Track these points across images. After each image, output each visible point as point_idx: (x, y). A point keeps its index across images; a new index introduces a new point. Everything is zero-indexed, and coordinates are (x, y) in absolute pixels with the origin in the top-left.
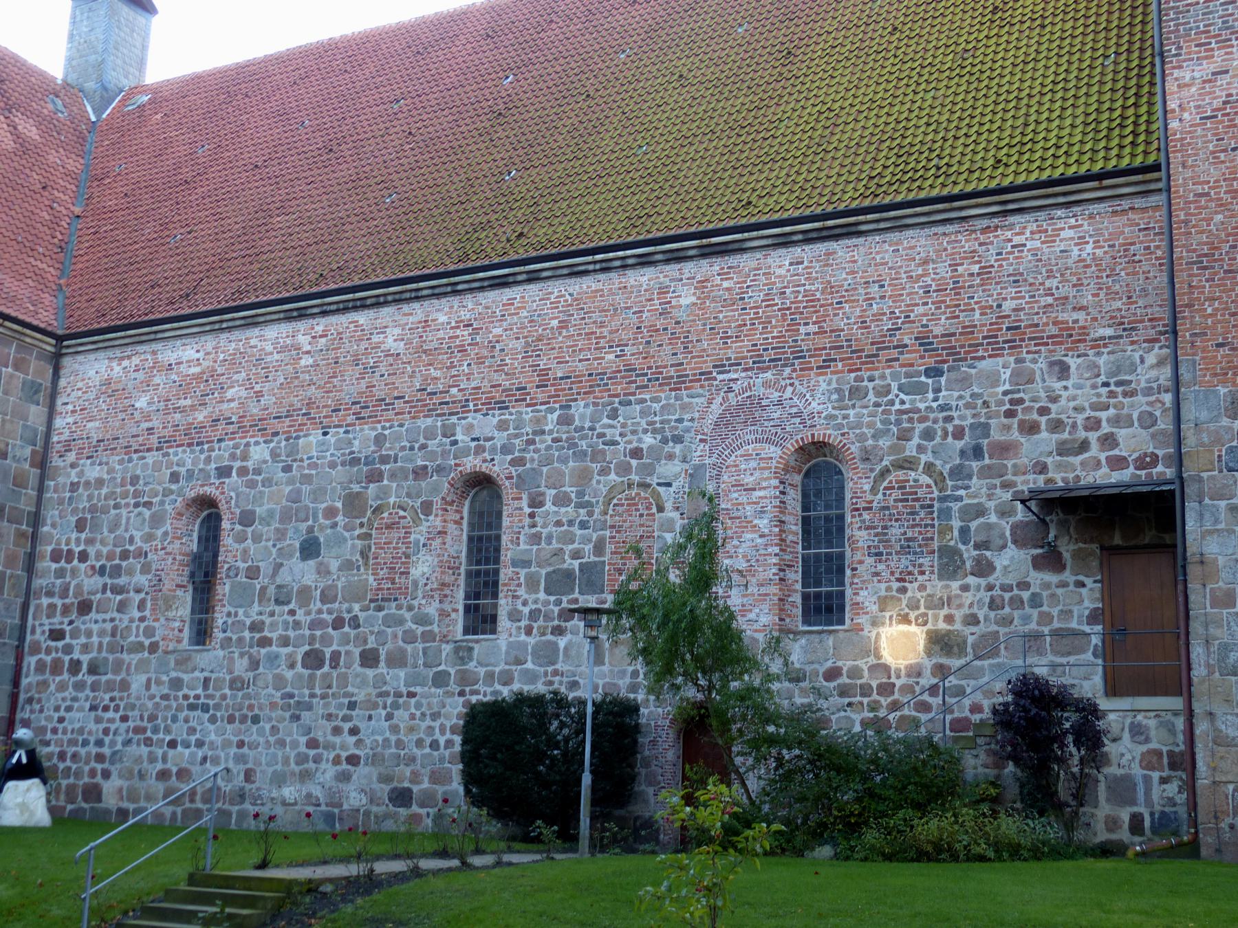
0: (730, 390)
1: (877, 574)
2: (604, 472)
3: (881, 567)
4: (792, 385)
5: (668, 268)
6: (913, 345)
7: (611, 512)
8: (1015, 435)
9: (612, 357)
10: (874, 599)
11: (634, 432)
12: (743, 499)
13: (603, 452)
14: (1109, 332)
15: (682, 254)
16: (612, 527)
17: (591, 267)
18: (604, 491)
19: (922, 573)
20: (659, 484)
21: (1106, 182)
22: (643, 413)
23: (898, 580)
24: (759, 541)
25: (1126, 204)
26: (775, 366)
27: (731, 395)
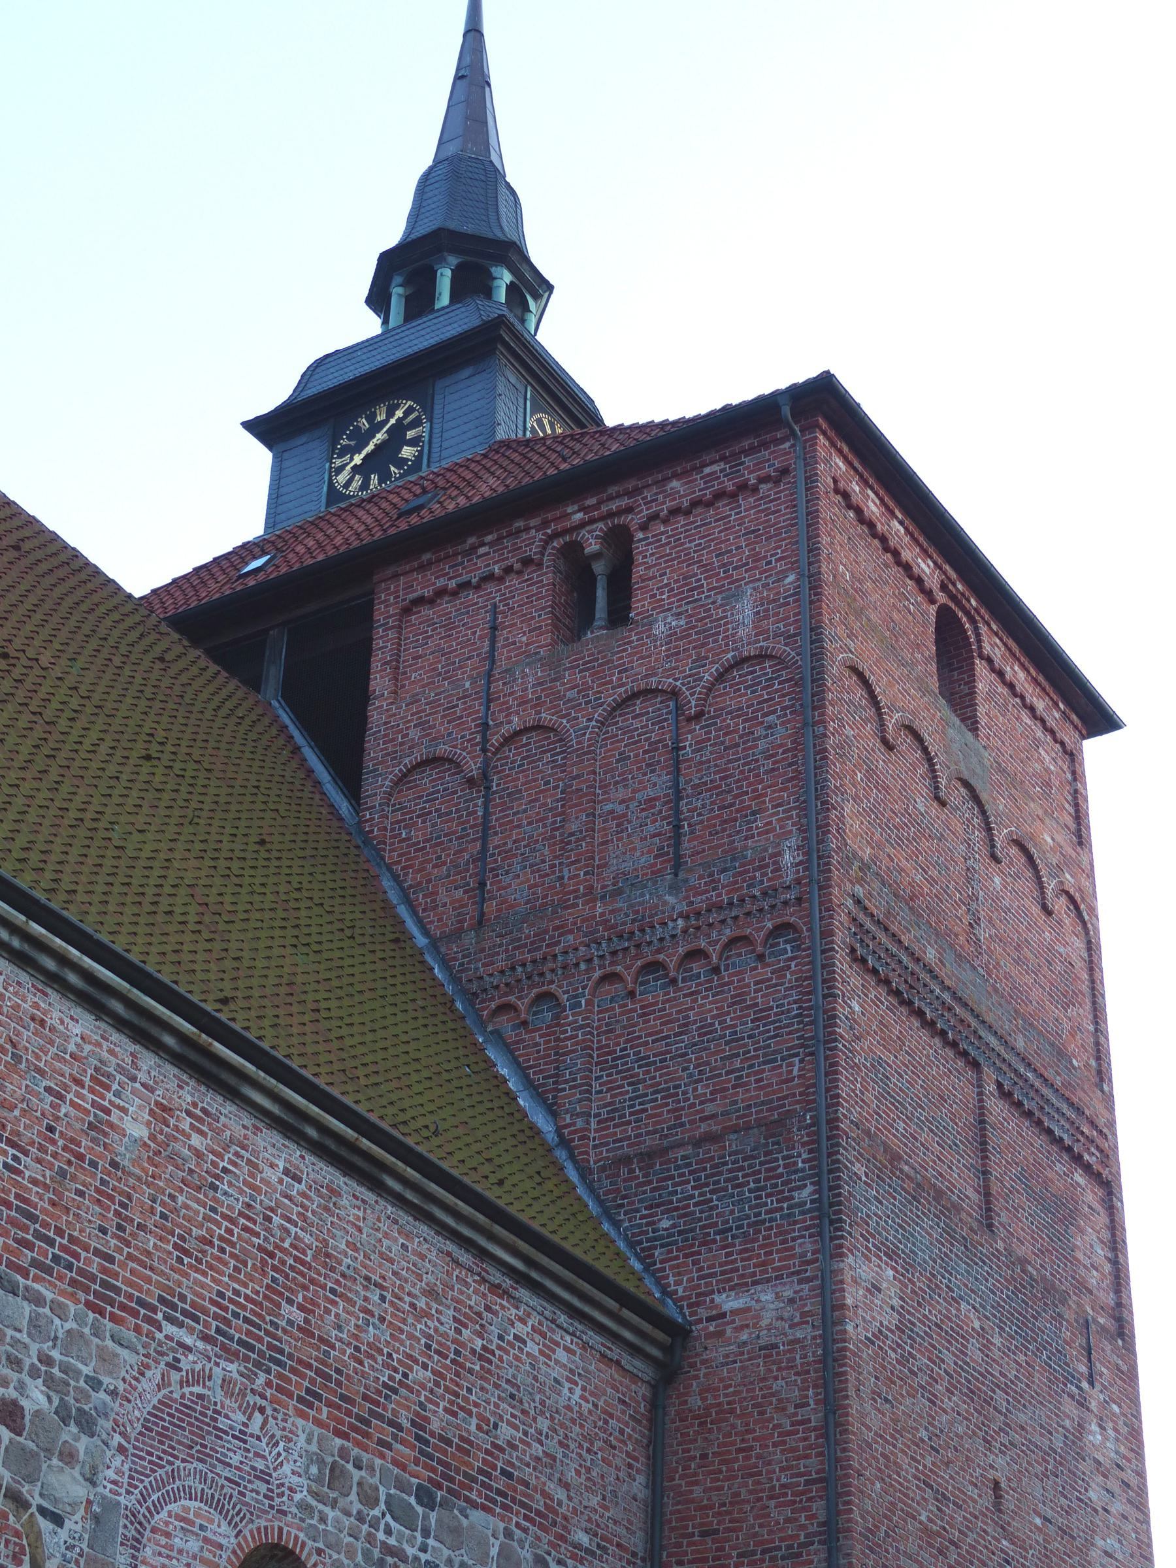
0: (174, 1366)
4: (262, 1410)
5: (115, 1037)
6: (409, 1432)
14: (584, 1539)
15: (155, 1031)
20: (42, 1511)
21: (626, 1313)
25: (615, 1353)
26: (246, 1359)
27: (175, 1376)
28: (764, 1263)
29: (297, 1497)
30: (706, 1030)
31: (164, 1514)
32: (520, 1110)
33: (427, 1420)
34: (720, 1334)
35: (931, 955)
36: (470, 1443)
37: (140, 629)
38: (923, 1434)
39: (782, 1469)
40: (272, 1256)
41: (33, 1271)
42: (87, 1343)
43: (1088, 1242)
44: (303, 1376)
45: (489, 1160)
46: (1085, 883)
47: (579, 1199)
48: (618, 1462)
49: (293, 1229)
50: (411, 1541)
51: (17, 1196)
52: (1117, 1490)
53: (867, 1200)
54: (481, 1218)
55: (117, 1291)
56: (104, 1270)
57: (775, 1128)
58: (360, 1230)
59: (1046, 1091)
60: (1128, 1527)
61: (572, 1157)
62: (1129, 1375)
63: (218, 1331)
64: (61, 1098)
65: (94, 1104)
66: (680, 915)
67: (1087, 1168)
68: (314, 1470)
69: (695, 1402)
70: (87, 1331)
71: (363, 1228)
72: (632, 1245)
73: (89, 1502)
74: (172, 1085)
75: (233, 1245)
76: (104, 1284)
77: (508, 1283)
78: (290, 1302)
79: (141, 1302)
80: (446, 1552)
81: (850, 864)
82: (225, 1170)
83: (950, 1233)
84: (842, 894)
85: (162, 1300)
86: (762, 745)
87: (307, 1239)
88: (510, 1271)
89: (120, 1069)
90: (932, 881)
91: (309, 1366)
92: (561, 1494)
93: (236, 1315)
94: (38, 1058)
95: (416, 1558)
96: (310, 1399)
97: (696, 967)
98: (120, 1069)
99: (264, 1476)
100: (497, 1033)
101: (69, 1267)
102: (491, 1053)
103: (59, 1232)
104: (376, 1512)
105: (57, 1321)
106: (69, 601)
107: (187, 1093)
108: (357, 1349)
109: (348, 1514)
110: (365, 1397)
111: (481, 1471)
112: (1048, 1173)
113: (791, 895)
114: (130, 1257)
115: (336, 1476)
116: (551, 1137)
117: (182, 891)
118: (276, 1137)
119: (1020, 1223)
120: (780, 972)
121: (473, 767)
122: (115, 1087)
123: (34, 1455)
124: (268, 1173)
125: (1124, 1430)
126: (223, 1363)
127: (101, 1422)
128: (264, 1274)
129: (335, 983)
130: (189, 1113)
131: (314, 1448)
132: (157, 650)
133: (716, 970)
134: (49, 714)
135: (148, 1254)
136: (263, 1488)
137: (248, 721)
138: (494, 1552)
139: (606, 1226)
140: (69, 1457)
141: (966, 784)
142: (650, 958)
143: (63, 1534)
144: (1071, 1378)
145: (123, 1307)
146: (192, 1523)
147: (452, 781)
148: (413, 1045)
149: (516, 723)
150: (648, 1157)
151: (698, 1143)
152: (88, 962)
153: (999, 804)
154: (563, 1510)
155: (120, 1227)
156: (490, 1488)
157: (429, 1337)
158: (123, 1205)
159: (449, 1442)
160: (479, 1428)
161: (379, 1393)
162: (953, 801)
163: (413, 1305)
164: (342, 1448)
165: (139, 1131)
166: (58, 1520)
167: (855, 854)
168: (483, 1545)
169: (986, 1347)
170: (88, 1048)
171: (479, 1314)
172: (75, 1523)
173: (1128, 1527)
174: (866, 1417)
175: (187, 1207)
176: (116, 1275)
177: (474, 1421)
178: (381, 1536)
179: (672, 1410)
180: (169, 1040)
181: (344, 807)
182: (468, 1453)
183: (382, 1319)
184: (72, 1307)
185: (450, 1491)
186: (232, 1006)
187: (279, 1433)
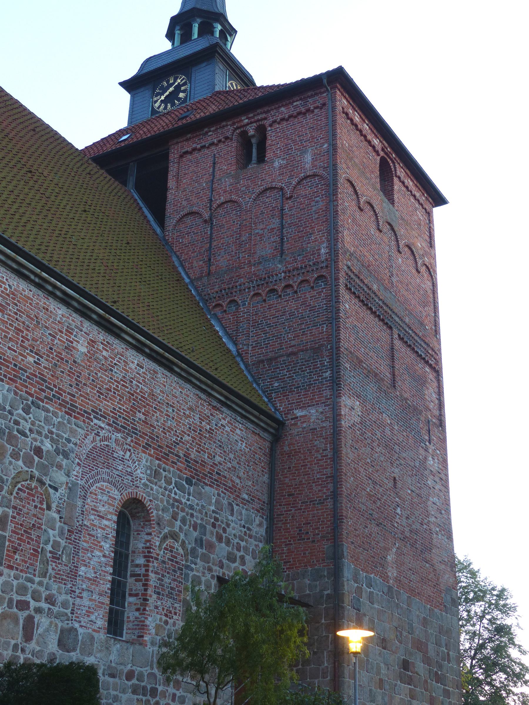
0: (98, 434)
1: (156, 607)
2: (15, 456)
3: (159, 603)
4: (130, 450)
5: (74, 315)
6: (183, 458)
7: (14, 493)
8: (214, 539)
9: (31, 360)
10: (154, 625)
11: (39, 433)
12: (96, 522)
13: (15, 436)
14: (246, 497)
15: (89, 313)
16: (15, 508)
17: (32, 277)
18: (13, 473)
19: (175, 614)
20: (50, 486)
21: (262, 417)
22: (47, 420)
23: (166, 615)
24: (103, 559)
25: (258, 431)
26: (124, 432)
27: (98, 438)
28: (312, 399)
29: (143, 481)
30: (292, 314)
31: (94, 487)
32: (224, 343)
33: (190, 454)
34: (295, 424)
35: (375, 287)
36: (205, 463)
37: (81, 162)
38: (369, 460)
39: (318, 473)
40: (133, 395)
41: (45, 400)
42: (66, 426)
43: (430, 392)
44: (144, 438)
45: (212, 361)
46: (432, 261)
47: (245, 375)
48: (258, 469)
49: (140, 386)
50: (184, 497)
51: (39, 373)
52: (438, 481)
53: (350, 376)
54: (209, 382)
55: (77, 407)
56: (71, 400)
57: (317, 350)
58: (165, 386)
59: (416, 338)
60: (442, 494)
61: (242, 360)
62: (443, 440)
63: (113, 422)
64: (55, 337)
65: (67, 339)
66: (283, 272)
67: (430, 366)
68: (149, 472)
69: (286, 448)
70: (65, 422)
71: (166, 386)
72: (264, 392)
73: (67, 483)
74: (96, 333)
75: (119, 391)
76: (71, 405)
77: (219, 405)
78: (140, 412)
79: (85, 412)
80: (196, 501)
81: (346, 253)
82: (115, 364)
83: (380, 388)
84: (342, 265)
85: (93, 411)
86: (314, 208)
87: (146, 389)
88: (220, 401)
89: (76, 327)
90: (376, 260)
91: (147, 435)
92: (238, 481)
93: (120, 416)
94: (46, 323)
95: (186, 503)
96: (147, 447)
97: (289, 291)
98: (76, 327)
99: (130, 474)
100: (215, 314)
101: (59, 399)
102: (213, 322)
103: (55, 386)
104: (171, 487)
105: (54, 418)
106: (54, 151)
107: (101, 336)
108: (164, 429)
109: (161, 487)
110: (167, 446)
111: (209, 473)
112: (416, 367)
113: (324, 265)
114: (81, 395)
115: (157, 474)
116: (234, 352)
117: (98, 261)
118: (134, 352)
119: (405, 385)
120: (319, 293)
121: (206, 216)
122: (75, 333)
123: (47, 466)
124: (131, 365)
125: (441, 460)
126: (115, 434)
127: (71, 454)
128: (130, 401)
129: (156, 296)
130: (102, 343)
131: (149, 464)
132: (88, 170)
133: (296, 292)
134: (47, 194)
135: (88, 394)
136: (130, 478)
137: (122, 198)
138: (214, 501)
139: (254, 385)
140: (60, 467)
141: (389, 224)
142: (272, 287)
143: (58, 494)
144: (423, 441)
145: (78, 413)
146: (104, 490)
147: (199, 221)
148: (184, 319)
149: (222, 199)
150: (270, 360)
151: (289, 355)
152: (64, 287)
153: (401, 231)
154: (238, 486)
155: (77, 384)
156: (212, 478)
157: (190, 425)
158: (78, 376)
159: (197, 462)
160: (208, 457)
161: (172, 444)
162: (384, 230)
163: (184, 413)
164: (159, 464)
165: (84, 350)
166: (56, 489)
167: (348, 250)
168: (210, 498)
169: (392, 430)
170: (64, 319)
171: (208, 417)
172: (62, 490)
173: (442, 494)
174: (348, 454)
175: (101, 377)
176: (76, 402)
177: (207, 455)
178: (173, 495)
179: (278, 452)
180: (94, 316)
181: (158, 230)
182: (204, 466)
183: (173, 418)
184: (60, 413)
185: (198, 479)
186: (117, 304)
187: (136, 459)
